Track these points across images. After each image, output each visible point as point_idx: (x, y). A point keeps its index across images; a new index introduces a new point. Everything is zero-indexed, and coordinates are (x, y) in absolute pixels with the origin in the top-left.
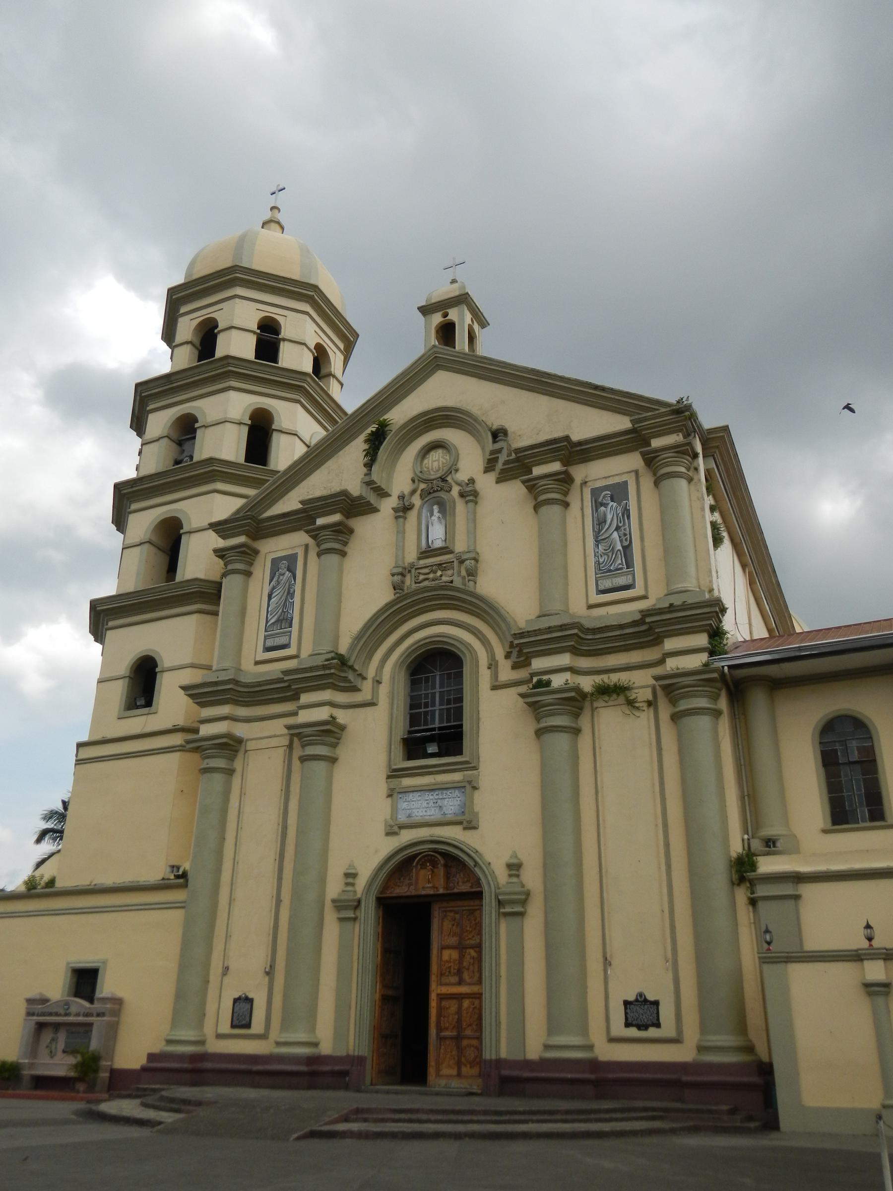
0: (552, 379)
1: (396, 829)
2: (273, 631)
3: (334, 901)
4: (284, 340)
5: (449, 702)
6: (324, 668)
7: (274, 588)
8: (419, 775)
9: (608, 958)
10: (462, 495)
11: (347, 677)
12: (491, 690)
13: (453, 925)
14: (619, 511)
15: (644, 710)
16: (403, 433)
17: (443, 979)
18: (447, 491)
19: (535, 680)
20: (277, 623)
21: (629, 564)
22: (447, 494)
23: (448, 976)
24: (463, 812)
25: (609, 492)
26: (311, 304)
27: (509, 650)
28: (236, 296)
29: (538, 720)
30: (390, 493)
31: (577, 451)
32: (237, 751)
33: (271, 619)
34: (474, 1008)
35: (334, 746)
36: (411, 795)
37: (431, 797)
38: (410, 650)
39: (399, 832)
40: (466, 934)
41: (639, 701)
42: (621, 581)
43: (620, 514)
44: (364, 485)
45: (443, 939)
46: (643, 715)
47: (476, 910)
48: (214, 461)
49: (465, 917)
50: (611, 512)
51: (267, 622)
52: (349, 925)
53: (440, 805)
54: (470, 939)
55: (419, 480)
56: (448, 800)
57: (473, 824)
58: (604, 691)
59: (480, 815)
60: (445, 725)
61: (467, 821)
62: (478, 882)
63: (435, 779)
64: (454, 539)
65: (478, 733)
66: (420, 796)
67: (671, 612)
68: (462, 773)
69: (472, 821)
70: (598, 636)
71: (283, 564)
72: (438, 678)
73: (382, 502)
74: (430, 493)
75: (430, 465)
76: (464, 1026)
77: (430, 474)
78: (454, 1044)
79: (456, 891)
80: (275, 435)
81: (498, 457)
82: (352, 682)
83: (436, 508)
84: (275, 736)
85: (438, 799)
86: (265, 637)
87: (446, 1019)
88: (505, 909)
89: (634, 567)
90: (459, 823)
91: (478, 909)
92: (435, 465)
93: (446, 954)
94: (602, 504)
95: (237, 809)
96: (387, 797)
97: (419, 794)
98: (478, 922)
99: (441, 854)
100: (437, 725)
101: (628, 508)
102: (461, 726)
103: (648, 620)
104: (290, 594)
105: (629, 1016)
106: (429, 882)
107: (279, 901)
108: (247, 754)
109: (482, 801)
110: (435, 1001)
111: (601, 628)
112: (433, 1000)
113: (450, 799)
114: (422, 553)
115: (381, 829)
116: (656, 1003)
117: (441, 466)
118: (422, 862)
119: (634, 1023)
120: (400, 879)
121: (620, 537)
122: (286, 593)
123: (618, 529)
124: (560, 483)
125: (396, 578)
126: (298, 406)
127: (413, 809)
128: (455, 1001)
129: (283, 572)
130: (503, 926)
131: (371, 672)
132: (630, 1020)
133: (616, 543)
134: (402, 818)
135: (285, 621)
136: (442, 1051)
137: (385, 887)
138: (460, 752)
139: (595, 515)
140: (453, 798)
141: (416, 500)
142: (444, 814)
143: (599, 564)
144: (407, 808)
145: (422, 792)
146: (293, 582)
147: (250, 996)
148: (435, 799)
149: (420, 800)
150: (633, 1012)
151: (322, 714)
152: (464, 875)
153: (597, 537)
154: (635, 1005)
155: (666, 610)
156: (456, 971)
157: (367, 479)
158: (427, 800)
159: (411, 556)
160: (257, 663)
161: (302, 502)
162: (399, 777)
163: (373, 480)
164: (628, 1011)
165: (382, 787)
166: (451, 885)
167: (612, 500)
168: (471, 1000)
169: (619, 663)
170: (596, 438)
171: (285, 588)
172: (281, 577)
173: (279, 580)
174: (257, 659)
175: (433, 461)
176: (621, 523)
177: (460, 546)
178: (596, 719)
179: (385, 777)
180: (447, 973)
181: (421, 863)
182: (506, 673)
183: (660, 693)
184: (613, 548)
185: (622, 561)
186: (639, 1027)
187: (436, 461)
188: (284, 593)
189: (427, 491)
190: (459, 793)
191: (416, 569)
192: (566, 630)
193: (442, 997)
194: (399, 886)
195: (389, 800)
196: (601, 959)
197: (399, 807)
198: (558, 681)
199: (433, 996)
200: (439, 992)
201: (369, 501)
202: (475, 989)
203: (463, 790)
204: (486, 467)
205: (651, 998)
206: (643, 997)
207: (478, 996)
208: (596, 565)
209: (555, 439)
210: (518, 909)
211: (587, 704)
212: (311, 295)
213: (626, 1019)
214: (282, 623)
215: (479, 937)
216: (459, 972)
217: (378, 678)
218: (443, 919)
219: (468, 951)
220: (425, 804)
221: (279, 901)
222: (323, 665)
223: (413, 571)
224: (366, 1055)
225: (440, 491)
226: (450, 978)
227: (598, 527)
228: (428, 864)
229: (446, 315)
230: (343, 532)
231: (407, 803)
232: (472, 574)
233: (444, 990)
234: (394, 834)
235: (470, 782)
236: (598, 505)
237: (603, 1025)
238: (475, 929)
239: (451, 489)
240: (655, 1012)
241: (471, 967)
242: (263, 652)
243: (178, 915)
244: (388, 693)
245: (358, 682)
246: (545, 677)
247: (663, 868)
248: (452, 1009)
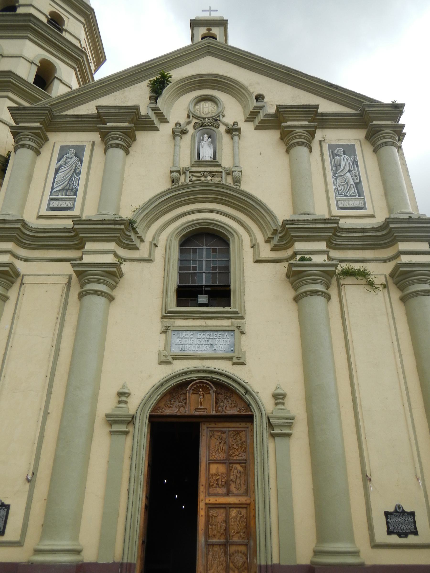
0: (298, 74)
1: (170, 359)
2: (58, 196)
3: (107, 416)
4: (66, 31)
5: (214, 268)
6: (115, 223)
7: (61, 166)
8: (192, 319)
9: (368, 475)
10: (229, 131)
11: (130, 236)
12: (254, 263)
13: (220, 443)
14: (350, 161)
15: (380, 290)
16: (182, 84)
17: (210, 490)
18: (216, 127)
19: (298, 257)
20: (62, 191)
21: (361, 194)
22: (216, 128)
23: (216, 487)
24: (232, 350)
25: (341, 149)
26: (86, 20)
27: (270, 236)
29: (295, 289)
30: (168, 120)
31: (319, 119)
32: (13, 283)
33: (55, 188)
34: (241, 517)
35: (113, 288)
36: (184, 333)
37: (203, 337)
38: (185, 226)
39: (172, 362)
40: (233, 451)
41: (375, 284)
43: (351, 163)
44: (150, 109)
45: (211, 455)
46: (380, 293)
47: (242, 431)
48: (11, 74)
49: (232, 436)
50: (344, 160)
51: (52, 189)
52: (122, 437)
53: (211, 343)
54: (235, 456)
55: (193, 116)
56: (218, 340)
57: (242, 360)
58: (346, 273)
59: (247, 354)
60: (211, 284)
61: (237, 358)
62: (248, 406)
63: (205, 323)
64: (221, 156)
65: (244, 292)
66: (192, 334)
67: (408, 222)
68: (230, 321)
69: (241, 358)
70: (344, 235)
71: (71, 151)
72: (205, 250)
73: (161, 125)
74: (202, 126)
75: (202, 109)
76: (231, 534)
77: (201, 114)
78: (222, 550)
79: (223, 413)
80: (56, 81)
81: (259, 112)
82: (133, 242)
83: (206, 136)
84: (53, 275)
85: (209, 338)
86: (50, 200)
87: (214, 527)
88: (274, 430)
89: (364, 196)
90: (230, 359)
91: (245, 431)
92: (206, 110)
93: (214, 468)
94: (337, 155)
95: (8, 330)
96: (161, 333)
97: (192, 333)
98: (244, 442)
99: (213, 382)
100: (204, 284)
101: (356, 160)
102: (229, 286)
103: (391, 225)
104: (76, 172)
105: (389, 525)
106: (201, 405)
107: (46, 414)
108: (23, 286)
110: (204, 510)
111: (349, 229)
112: (202, 509)
113: (220, 340)
114: (195, 162)
115: (155, 359)
116: (412, 514)
117: (210, 111)
118: (194, 388)
119: (395, 531)
120: (170, 401)
121: (352, 177)
122: (72, 171)
123: (350, 171)
124: (309, 134)
125: (175, 174)
126: (73, 71)
127: (185, 344)
128: (222, 510)
129: (70, 156)
130: (271, 445)
131: (148, 237)
132: (391, 529)
133: (349, 180)
134: (175, 351)
135: (70, 190)
136: (210, 557)
137: (156, 408)
138: (229, 305)
139: (333, 161)
140: (223, 339)
141: (190, 128)
142: (215, 351)
143: (338, 190)
144: (179, 343)
145: (194, 332)
146: (80, 164)
147: (6, 503)
148: (207, 338)
149: (193, 338)
150: (394, 522)
152: (232, 401)
153: (335, 174)
154: (394, 515)
155: (407, 220)
156: (223, 483)
157: (153, 105)
158: (199, 338)
160: (39, 217)
161: (98, 108)
162: (172, 319)
163: (158, 107)
164: (389, 520)
166: (220, 408)
167: (344, 153)
168: (238, 509)
169: (356, 257)
170: (334, 113)
171: (71, 168)
172: (69, 160)
173: (66, 161)
174: (41, 214)
175: (203, 108)
176: (352, 168)
178: (343, 292)
179: (159, 316)
180: (215, 485)
181: (193, 388)
183: (390, 281)
184: (347, 183)
185: (355, 191)
186: (400, 535)
188: (71, 170)
189: (200, 123)
190: (228, 335)
191: (190, 172)
192: (328, 223)
193: (210, 507)
194: (169, 407)
195: (163, 335)
196: (360, 476)
197: (173, 341)
198: (317, 259)
199: (202, 506)
200: (207, 501)
201: (153, 121)
202: (243, 500)
203: (232, 334)
204: (247, 117)
205: (407, 509)
206: (401, 508)
207: (245, 506)
208: (336, 191)
209: (309, 105)
210: (286, 431)
211: (334, 281)
212: (88, 13)
213: (388, 527)
214: (67, 191)
215: (245, 454)
216: (227, 484)
217: (155, 242)
218: (210, 437)
219: (234, 465)
220: (197, 341)
221: (46, 414)
222: (115, 221)
223: (188, 173)
224: (135, 562)
225: (210, 126)
226: (218, 489)
227: (335, 168)
228: (201, 390)
229: (209, 30)
231: (180, 339)
232: (237, 181)
233: (213, 500)
234: (169, 363)
235: (238, 327)
236: (334, 155)
237: (366, 532)
238: (241, 447)
239: (219, 126)
240: (412, 521)
241: (238, 481)
242: (46, 210)
244: (163, 254)
245: (137, 242)
246: (307, 256)
247: (407, 406)
248: (220, 517)
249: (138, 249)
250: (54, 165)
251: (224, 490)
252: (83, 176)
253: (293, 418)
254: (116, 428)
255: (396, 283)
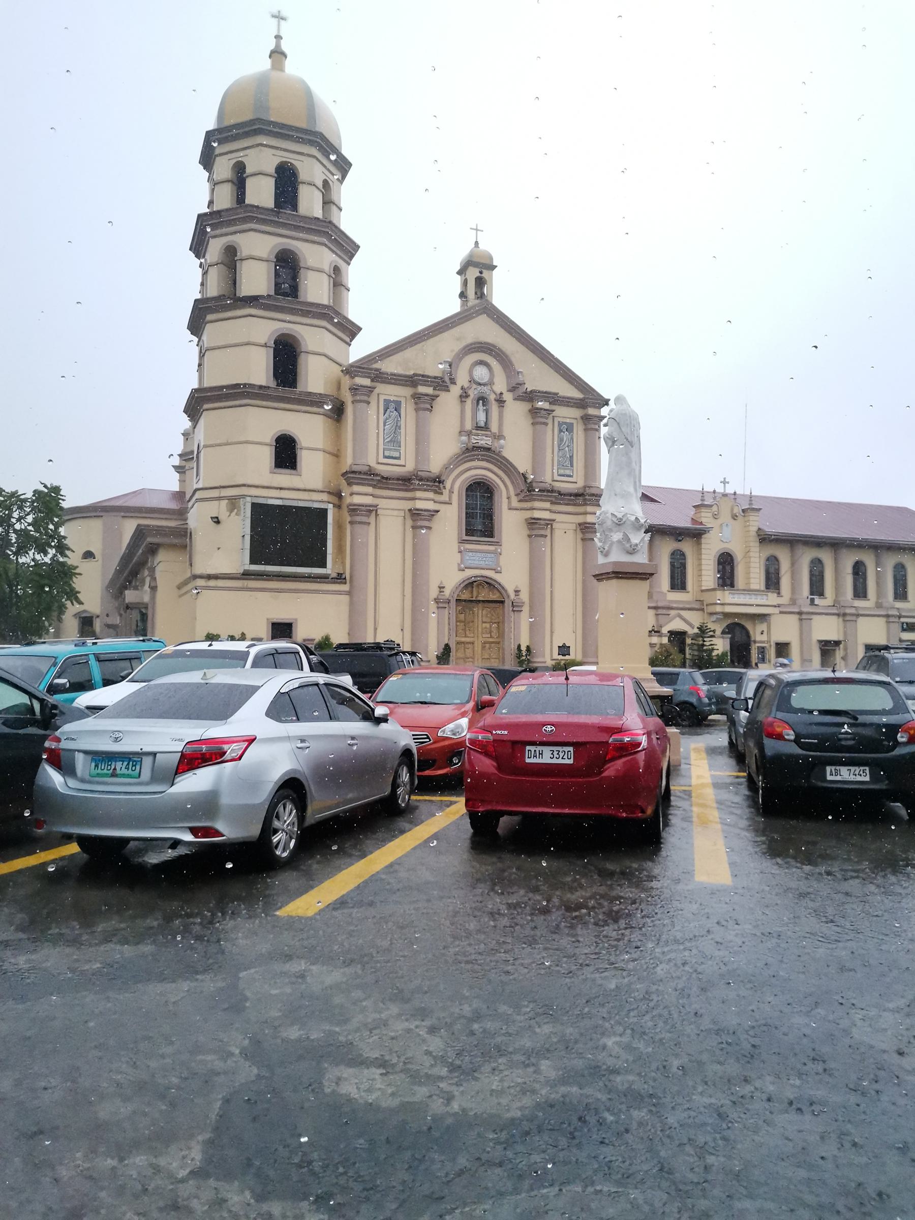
3: (435, 599)
7: (387, 419)
10: (496, 400)
14: (569, 437)
21: (572, 465)
28: (314, 157)
42: (568, 472)
50: (566, 435)
52: (443, 609)
93: (484, 625)
109: (503, 560)
123: (568, 446)
131: (448, 484)
134: (468, 563)
151: (430, 506)
159: (468, 426)
160: (379, 463)
165: (455, 545)
177: (494, 428)
182: (515, 503)
187: (481, 373)
229: (481, 273)
230: (434, 398)
243: (346, 598)
249: (442, 494)
250: (382, 418)
251: (489, 636)
252: (403, 430)
253: (524, 603)
254: (441, 605)
255: (581, 529)
